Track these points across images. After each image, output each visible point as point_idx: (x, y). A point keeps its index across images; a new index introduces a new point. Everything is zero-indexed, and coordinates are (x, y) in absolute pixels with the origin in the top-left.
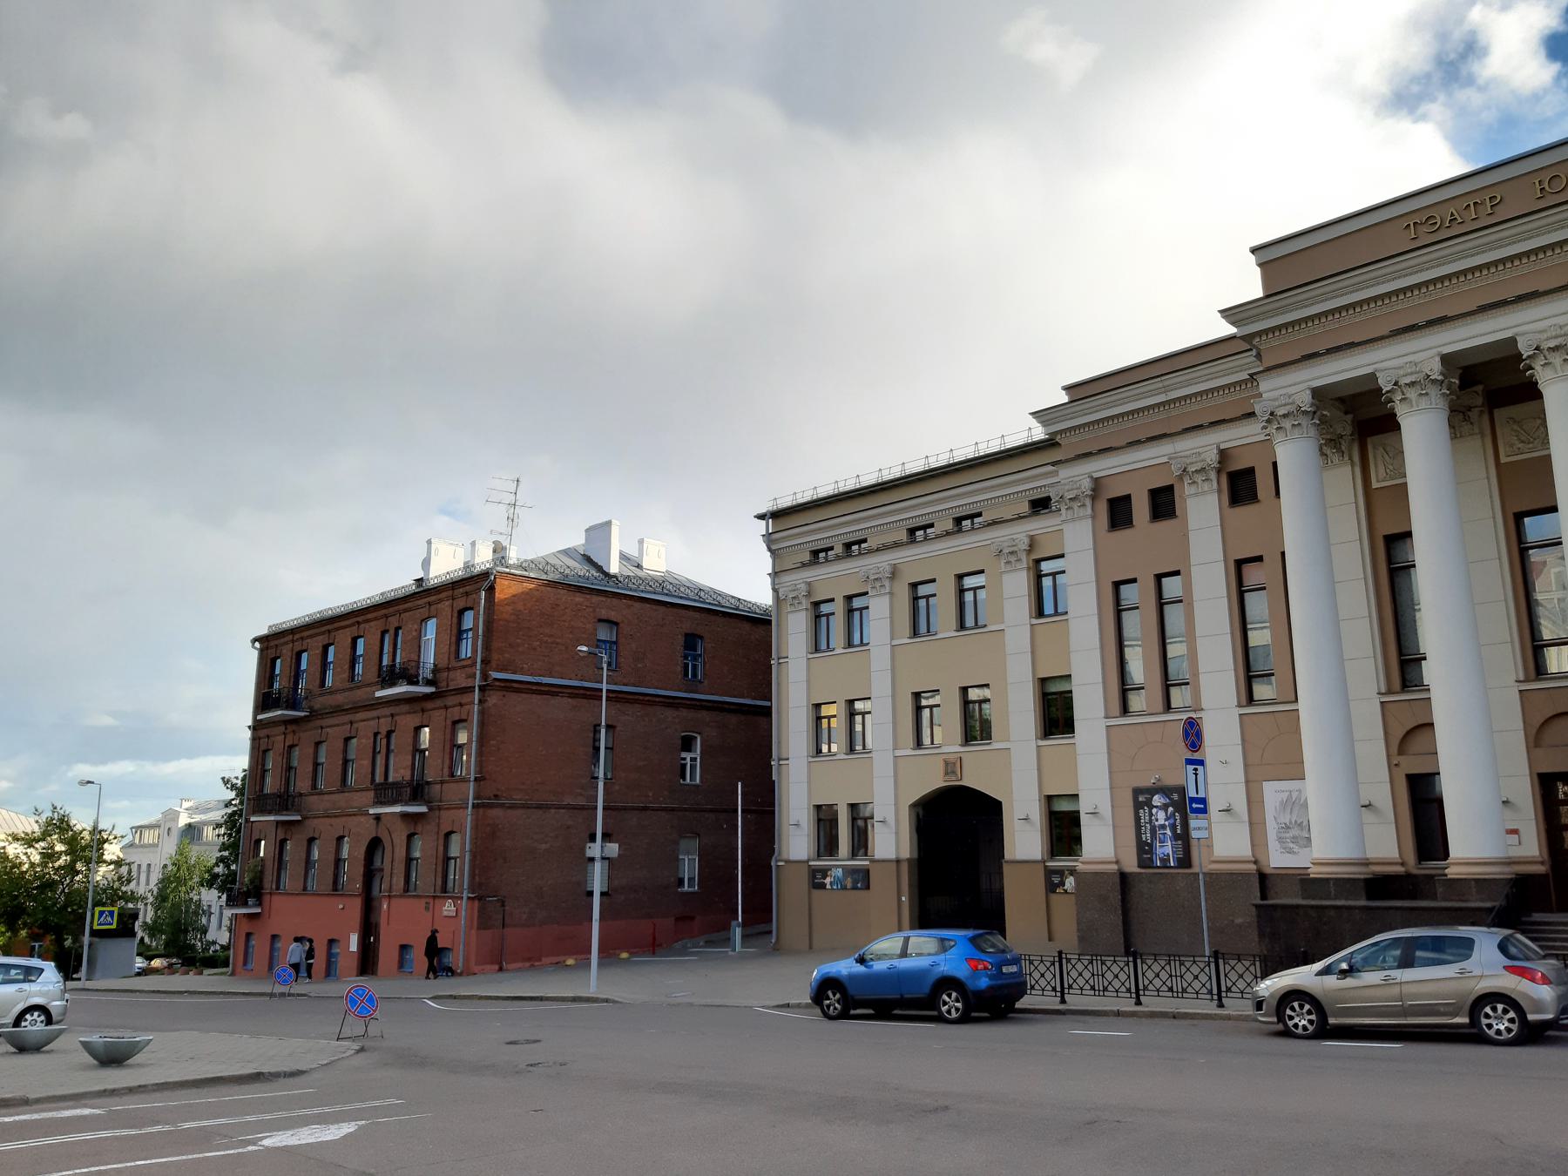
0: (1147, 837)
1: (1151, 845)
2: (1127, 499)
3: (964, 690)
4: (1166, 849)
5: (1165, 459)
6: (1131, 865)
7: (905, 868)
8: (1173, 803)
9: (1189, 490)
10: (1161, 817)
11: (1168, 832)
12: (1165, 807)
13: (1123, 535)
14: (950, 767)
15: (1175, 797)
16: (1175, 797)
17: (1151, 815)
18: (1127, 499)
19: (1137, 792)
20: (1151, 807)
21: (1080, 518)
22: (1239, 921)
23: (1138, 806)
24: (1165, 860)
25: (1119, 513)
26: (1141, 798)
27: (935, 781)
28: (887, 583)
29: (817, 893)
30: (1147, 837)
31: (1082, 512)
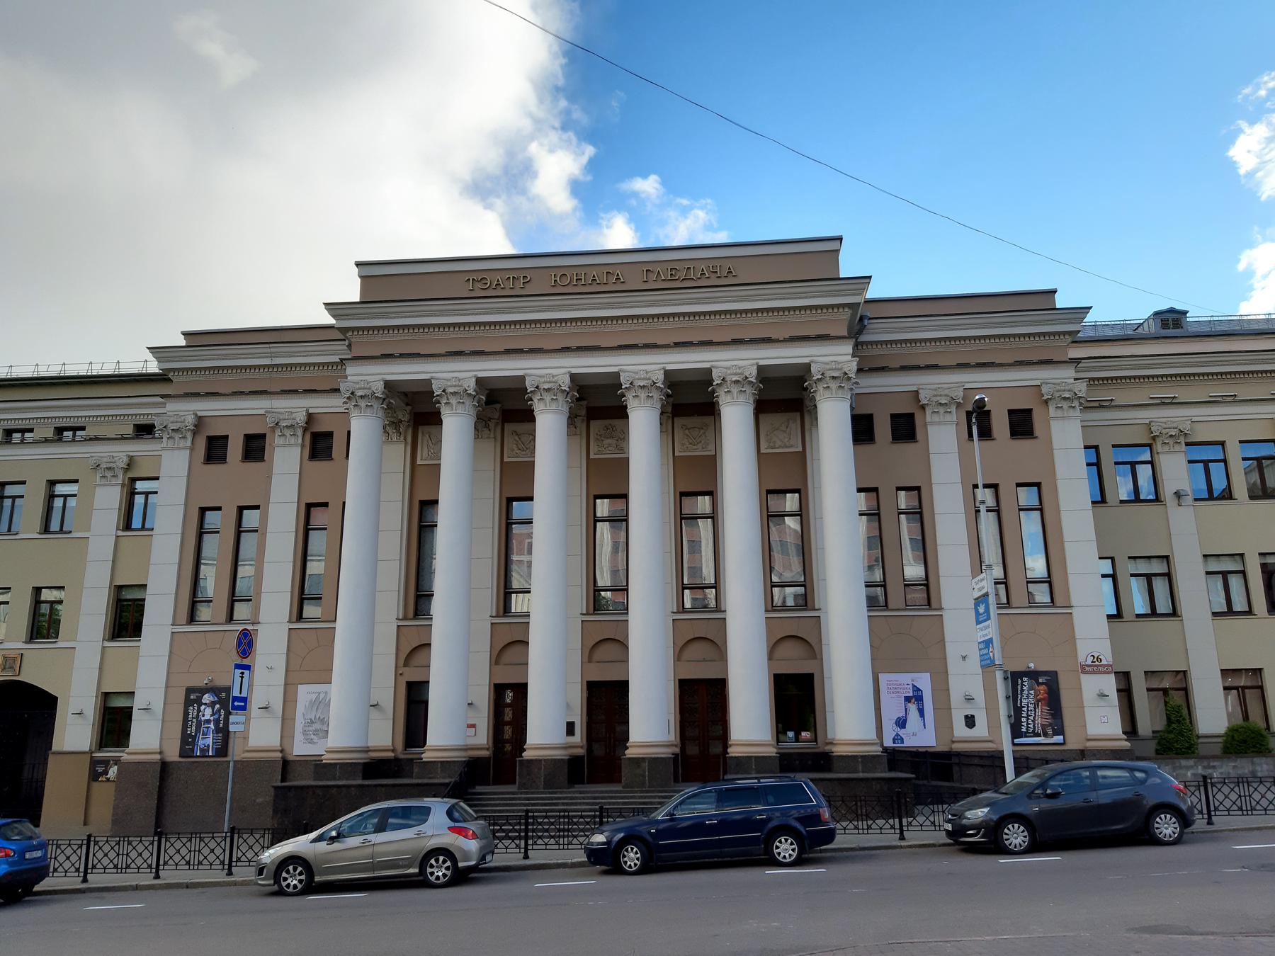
0: (192, 730)
1: (194, 738)
4: (207, 741)
5: (262, 412)
6: (173, 755)
8: (220, 701)
9: (278, 440)
10: (207, 713)
11: (212, 726)
12: (212, 704)
17: (199, 711)
19: (189, 691)
20: (200, 704)
21: (179, 448)
22: (259, 800)
23: (188, 703)
24: (204, 751)
25: (215, 449)
26: (193, 697)
30: (192, 730)
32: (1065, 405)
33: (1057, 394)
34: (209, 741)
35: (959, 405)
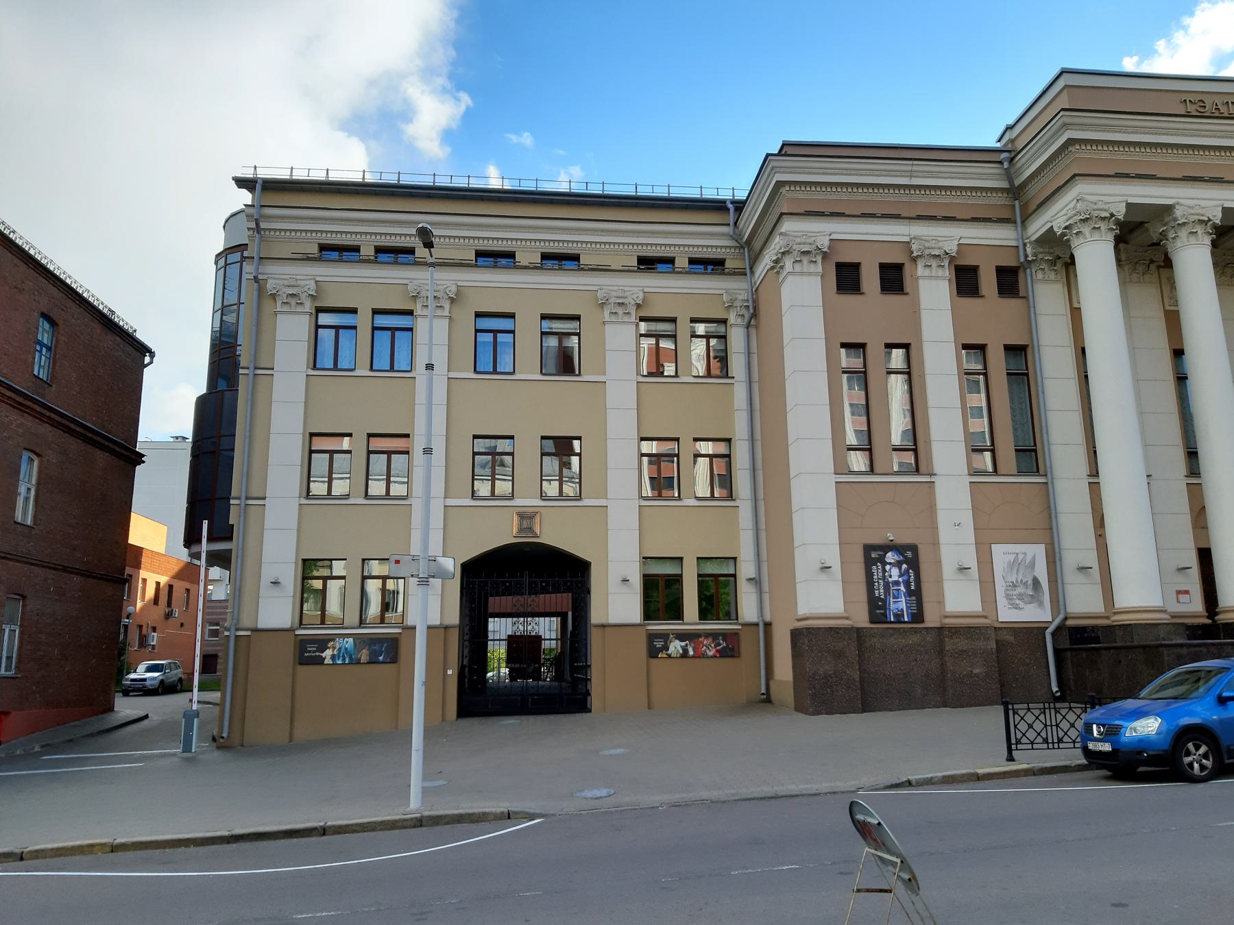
1: (884, 601)
2: (856, 267)
3: (579, 438)
4: (900, 604)
5: (907, 239)
6: (861, 618)
7: (454, 637)
8: (906, 561)
9: (921, 270)
10: (895, 574)
11: (902, 588)
13: (850, 300)
14: (526, 518)
15: (909, 554)
16: (909, 554)
17: (884, 571)
18: (856, 267)
19: (868, 549)
20: (884, 563)
21: (810, 274)
23: (869, 563)
24: (899, 616)
25: (847, 278)
26: (873, 554)
27: (499, 532)
28: (447, 305)
29: (304, 671)
31: (812, 268)
32: (934, 263)
33: (927, 252)
34: (902, 604)
35: (952, 259)
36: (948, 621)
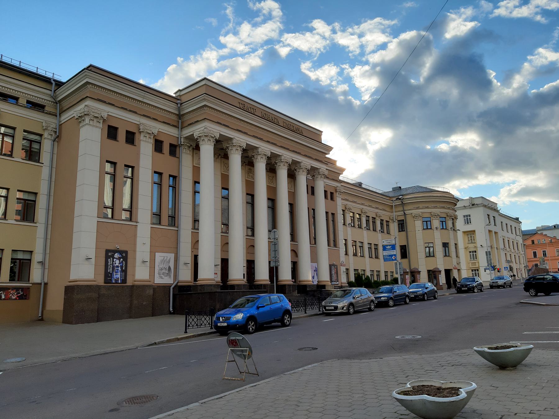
0: (110, 270)
1: (111, 274)
4: (118, 276)
8: (123, 257)
9: (142, 137)
10: (117, 262)
11: (120, 269)
12: (119, 259)
15: (124, 255)
16: (124, 255)
17: (113, 261)
19: (107, 251)
22: (144, 303)
23: (107, 257)
24: (116, 281)
25: (112, 133)
26: (109, 254)
30: (110, 270)
32: (148, 136)
33: (146, 131)
34: (119, 276)
36: (136, 283)
